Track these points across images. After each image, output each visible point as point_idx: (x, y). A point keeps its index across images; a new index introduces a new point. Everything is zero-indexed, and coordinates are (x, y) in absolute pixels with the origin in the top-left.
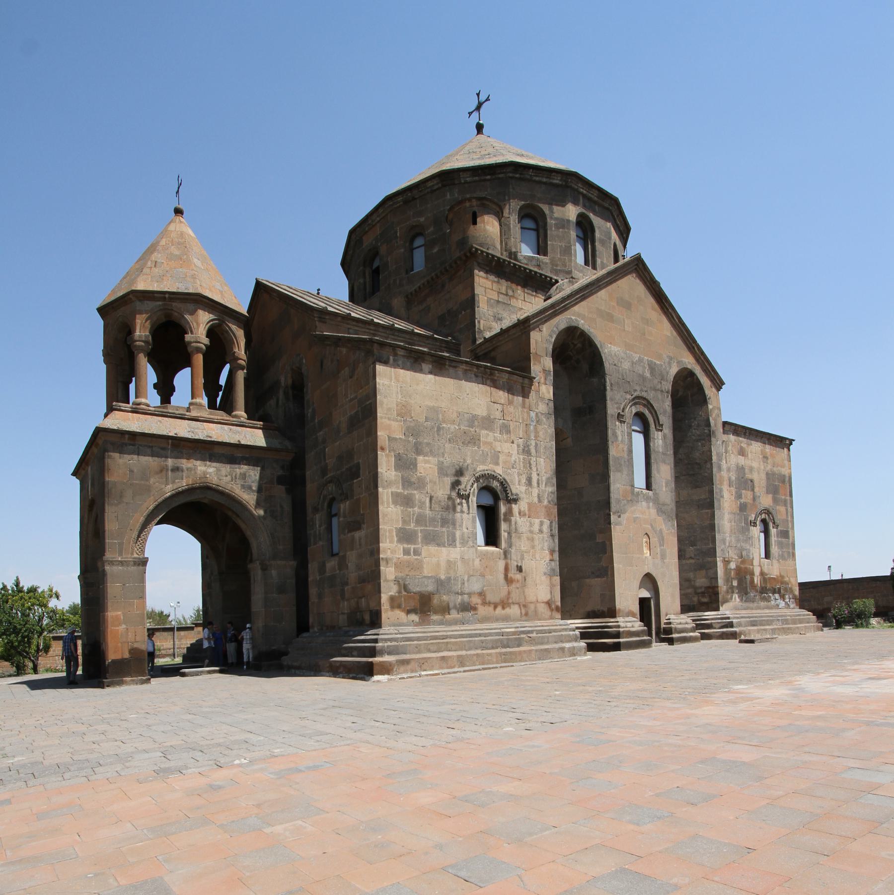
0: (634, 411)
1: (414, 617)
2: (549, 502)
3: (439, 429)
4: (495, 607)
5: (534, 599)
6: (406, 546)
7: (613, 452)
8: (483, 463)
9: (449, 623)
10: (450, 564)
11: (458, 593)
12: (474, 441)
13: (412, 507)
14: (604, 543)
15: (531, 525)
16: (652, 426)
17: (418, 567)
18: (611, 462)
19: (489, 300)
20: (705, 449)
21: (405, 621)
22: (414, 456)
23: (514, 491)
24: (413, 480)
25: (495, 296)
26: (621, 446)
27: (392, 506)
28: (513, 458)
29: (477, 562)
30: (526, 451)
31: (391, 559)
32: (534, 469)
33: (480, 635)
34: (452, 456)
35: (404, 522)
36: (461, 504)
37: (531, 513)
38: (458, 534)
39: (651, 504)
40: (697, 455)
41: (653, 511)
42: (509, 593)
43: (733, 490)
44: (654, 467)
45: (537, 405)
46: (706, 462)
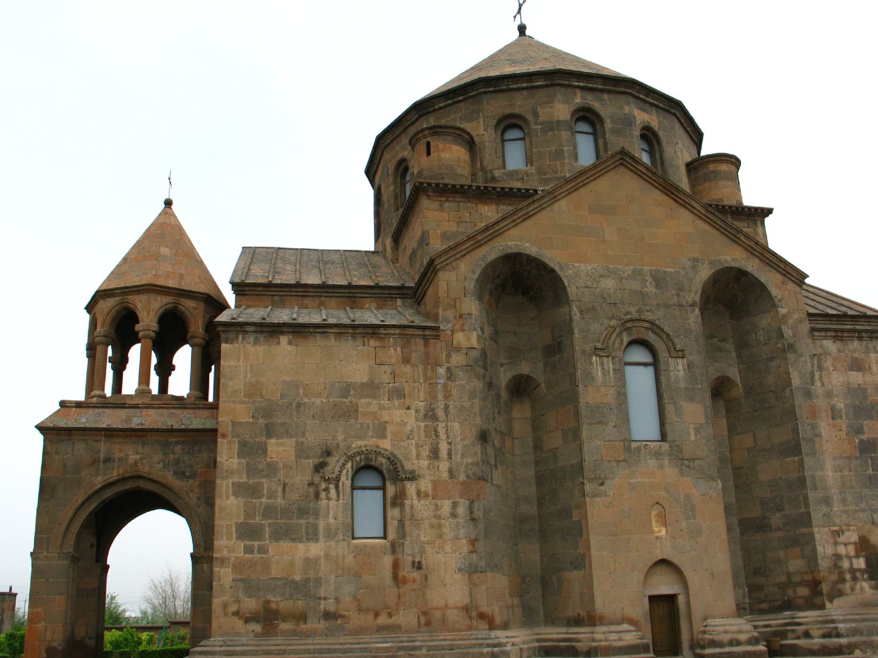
0: (626, 339)
1: (258, 628)
2: (468, 476)
3: (299, 405)
4: (377, 615)
5: (442, 604)
6: (248, 543)
7: (588, 397)
8: (362, 438)
9: (308, 634)
10: (310, 563)
11: (320, 598)
12: (349, 413)
13: (260, 498)
14: (580, 521)
15: (437, 508)
16: (663, 354)
17: (266, 566)
18: (583, 412)
20: (782, 370)
21: (243, 631)
23: (408, 466)
24: (260, 467)
25: (453, 227)
26: (603, 389)
27: (232, 498)
28: (409, 428)
29: (350, 560)
30: (430, 415)
31: (228, 559)
32: (443, 436)
33: (335, 651)
34: (316, 435)
35: (247, 515)
36: (327, 490)
37: (438, 490)
38: (321, 524)
39: (666, 461)
40: (770, 379)
41: (671, 473)
42: (399, 597)
43: (843, 423)
44: (669, 408)
45: (448, 356)
46: (783, 390)
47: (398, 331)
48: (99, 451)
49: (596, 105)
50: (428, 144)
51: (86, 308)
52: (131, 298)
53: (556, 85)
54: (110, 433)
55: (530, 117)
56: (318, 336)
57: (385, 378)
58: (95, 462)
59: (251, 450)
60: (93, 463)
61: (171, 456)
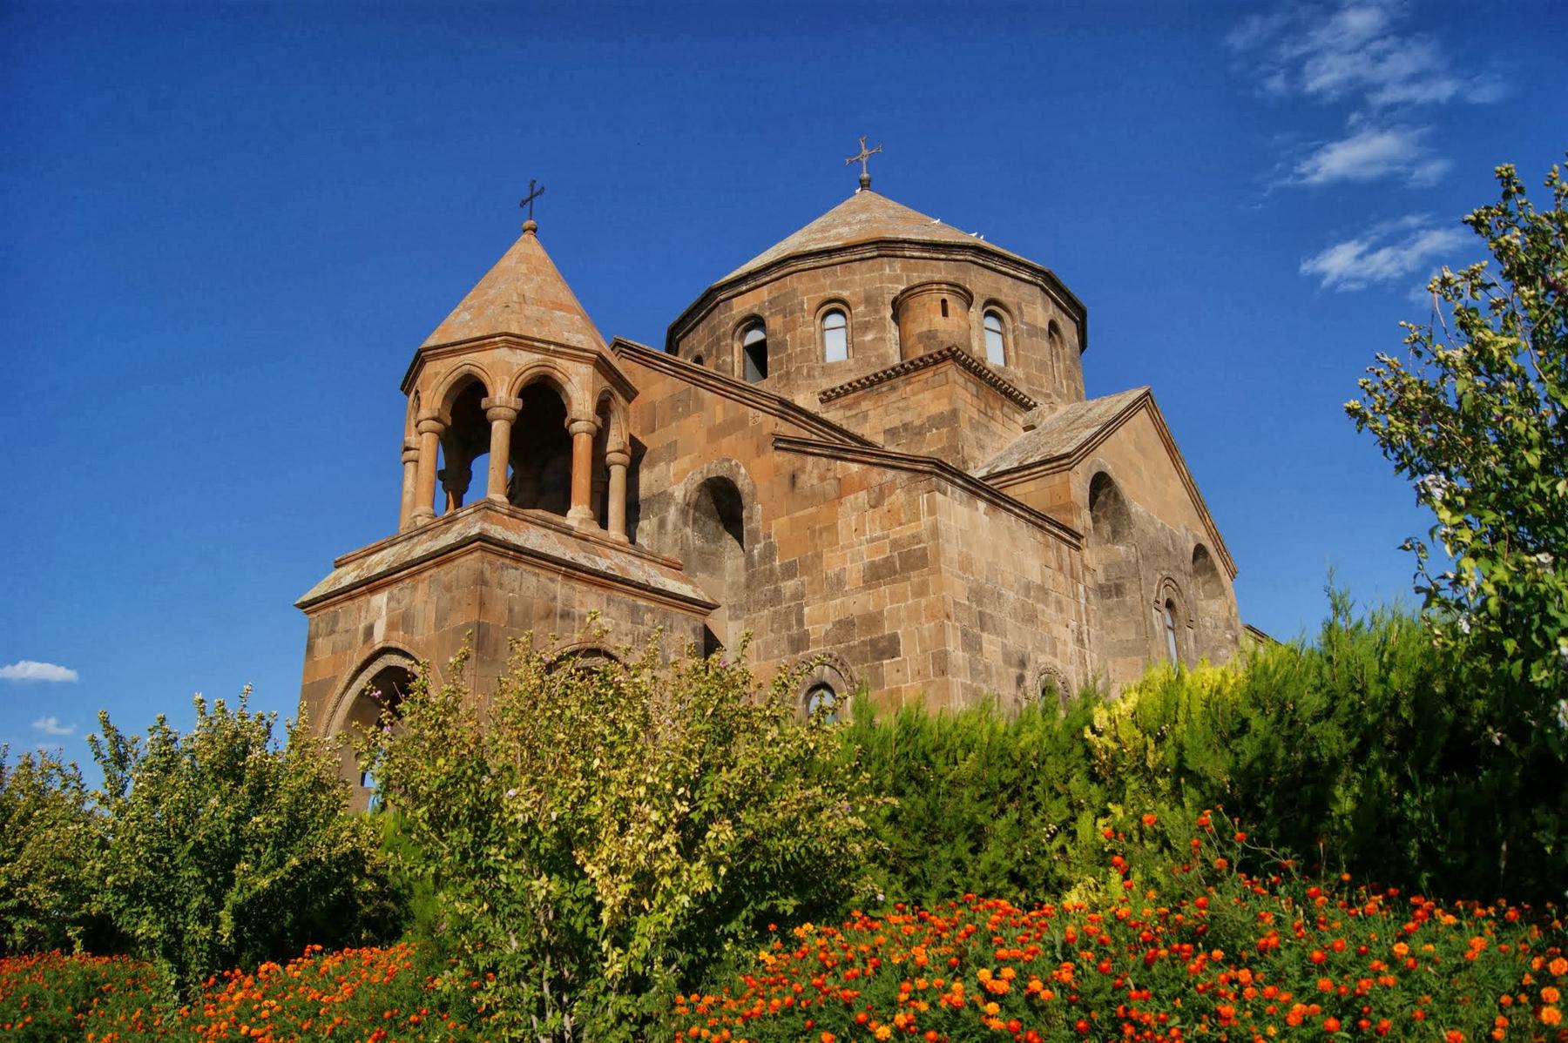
8: (1043, 651)
12: (1031, 618)
19: (971, 418)
22: (977, 630)
30: (1080, 641)
47: (1056, 531)
48: (555, 598)
49: (1060, 324)
50: (944, 301)
51: (420, 351)
52: (562, 363)
53: (1036, 285)
54: (571, 570)
55: (1016, 313)
56: (1004, 514)
57: (1049, 584)
58: (549, 614)
59: (972, 644)
60: (548, 616)
61: (643, 629)
